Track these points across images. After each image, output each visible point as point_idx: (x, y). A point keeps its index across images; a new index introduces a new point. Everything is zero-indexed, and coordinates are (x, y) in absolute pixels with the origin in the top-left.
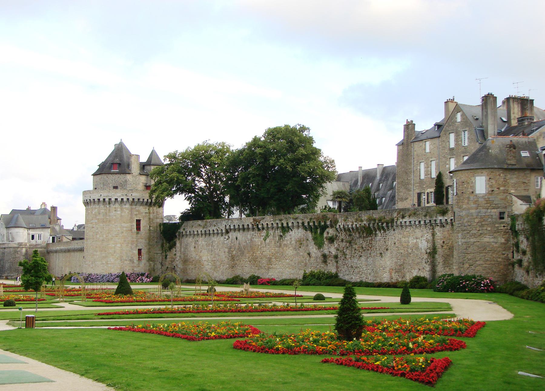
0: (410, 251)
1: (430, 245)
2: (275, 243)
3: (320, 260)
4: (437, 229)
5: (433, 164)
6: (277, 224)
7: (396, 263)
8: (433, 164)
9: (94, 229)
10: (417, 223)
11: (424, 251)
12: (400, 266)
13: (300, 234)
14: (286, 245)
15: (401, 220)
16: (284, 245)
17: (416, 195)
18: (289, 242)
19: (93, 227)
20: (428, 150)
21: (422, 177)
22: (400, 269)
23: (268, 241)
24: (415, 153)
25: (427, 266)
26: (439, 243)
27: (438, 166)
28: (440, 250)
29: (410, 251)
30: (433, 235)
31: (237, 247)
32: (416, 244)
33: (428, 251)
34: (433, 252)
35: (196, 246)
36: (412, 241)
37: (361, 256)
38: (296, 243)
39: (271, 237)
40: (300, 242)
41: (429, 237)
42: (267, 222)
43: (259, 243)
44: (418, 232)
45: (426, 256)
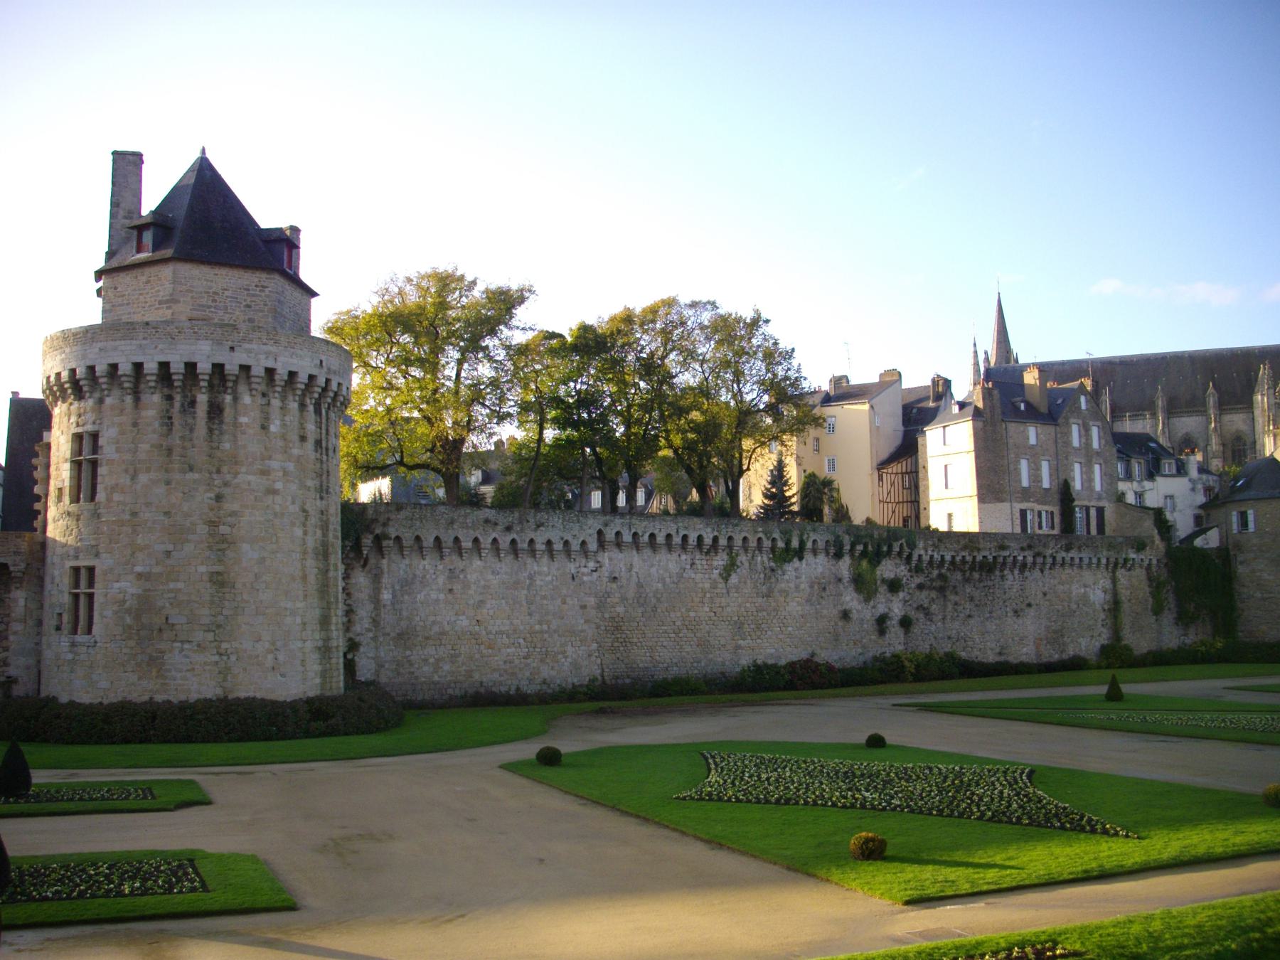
0: (1074, 607)
1: (1108, 597)
2: (755, 587)
3: (870, 626)
4: (1120, 573)
5: (1045, 466)
6: (774, 540)
7: (1047, 628)
8: (1045, 466)
9: (278, 499)
10: (1094, 560)
11: (1098, 607)
12: (1055, 632)
13: (820, 569)
14: (785, 593)
15: (1064, 554)
16: (781, 591)
17: (1018, 515)
18: (792, 585)
19: (275, 492)
20: (1033, 441)
21: (1025, 483)
22: (1056, 637)
23: (734, 579)
24: (1011, 441)
25: (1105, 630)
26: (1124, 594)
27: (1055, 471)
28: (1125, 606)
29: (1074, 607)
30: (1114, 581)
31: (631, 594)
32: (1085, 596)
33: (1106, 607)
34: (1115, 607)
35: (457, 587)
36: (1077, 590)
37: (970, 616)
38: (811, 587)
39: (744, 570)
40: (820, 587)
41: (1108, 584)
42: (744, 534)
43: (707, 585)
44: (1088, 576)
45: (1102, 616)
